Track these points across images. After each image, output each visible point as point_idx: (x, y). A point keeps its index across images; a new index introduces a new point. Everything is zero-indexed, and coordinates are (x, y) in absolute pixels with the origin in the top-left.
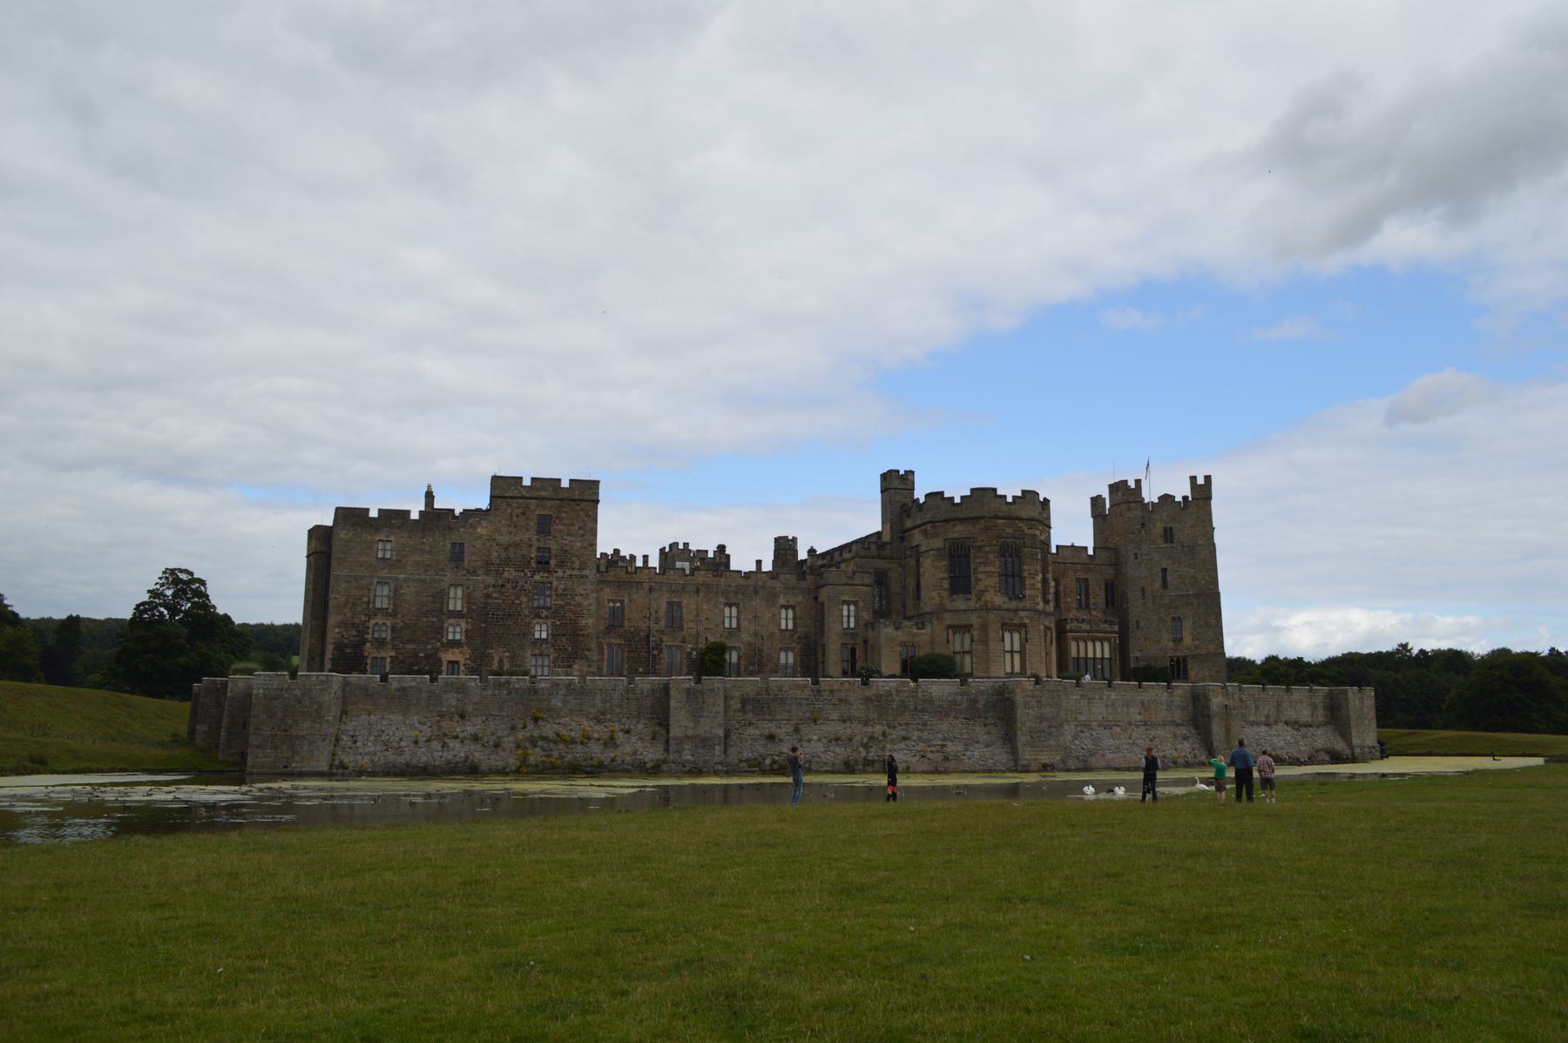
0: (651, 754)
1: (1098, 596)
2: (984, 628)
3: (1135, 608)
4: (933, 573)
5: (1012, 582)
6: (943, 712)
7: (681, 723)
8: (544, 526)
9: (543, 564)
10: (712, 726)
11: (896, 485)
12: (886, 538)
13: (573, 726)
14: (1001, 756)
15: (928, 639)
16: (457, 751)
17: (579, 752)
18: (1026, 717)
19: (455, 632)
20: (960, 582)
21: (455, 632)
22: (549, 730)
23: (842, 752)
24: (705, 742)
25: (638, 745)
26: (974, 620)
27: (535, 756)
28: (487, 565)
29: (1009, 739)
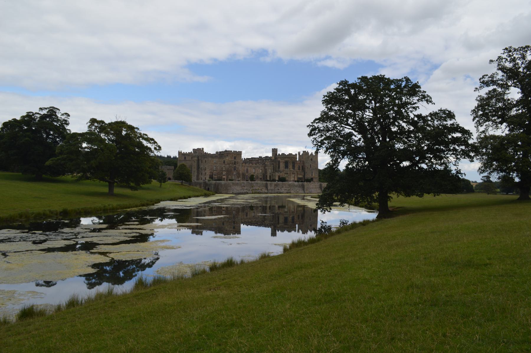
0: (266, 191)
1: (301, 169)
2: (290, 174)
3: (306, 170)
4: (282, 165)
5: (294, 167)
6: (296, 186)
7: (269, 188)
8: (235, 158)
9: (235, 163)
10: (273, 188)
11: (275, 151)
12: (273, 158)
13: (257, 188)
14: (303, 192)
15: (282, 175)
16: (245, 191)
17: (258, 191)
18: (306, 187)
19: (224, 173)
20: (287, 167)
21: (224, 173)
22: (254, 188)
23: (286, 191)
24: (272, 190)
25: (264, 190)
26: (289, 172)
27: (254, 191)
28: (228, 164)
29: (304, 190)
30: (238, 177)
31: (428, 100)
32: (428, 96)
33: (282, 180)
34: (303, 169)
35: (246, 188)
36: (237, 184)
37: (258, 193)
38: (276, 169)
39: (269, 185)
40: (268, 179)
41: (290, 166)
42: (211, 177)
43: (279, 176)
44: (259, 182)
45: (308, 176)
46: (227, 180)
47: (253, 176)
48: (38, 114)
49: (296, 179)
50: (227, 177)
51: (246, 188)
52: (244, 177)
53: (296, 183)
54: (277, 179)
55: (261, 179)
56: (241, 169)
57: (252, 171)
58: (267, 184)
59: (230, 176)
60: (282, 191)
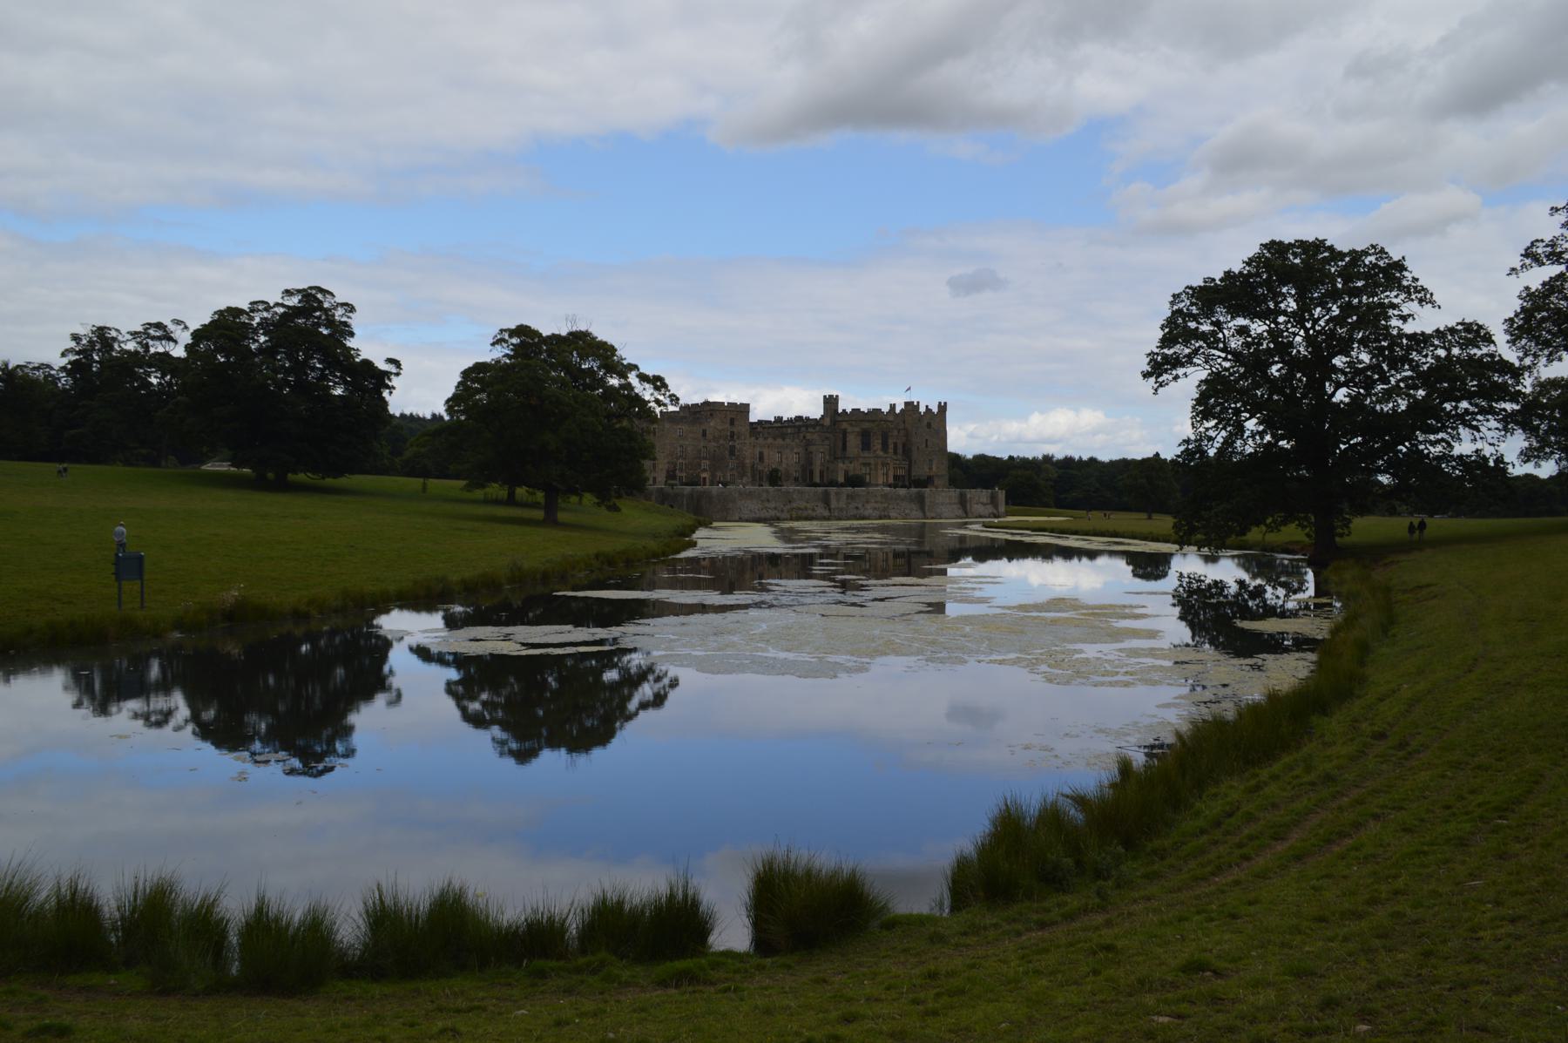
0: (826, 513)
1: (900, 451)
4: (853, 442)
7: (834, 504)
8: (732, 422)
10: (842, 504)
11: (831, 402)
12: (827, 422)
13: (803, 504)
14: (920, 514)
15: (855, 468)
16: (772, 513)
17: (805, 514)
18: (927, 501)
19: (705, 464)
20: (866, 446)
23: (877, 513)
24: (841, 510)
25: (821, 511)
29: (922, 508)
30: (742, 476)
31: (1425, 298)
32: (1423, 289)
33: (854, 481)
34: (907, 452)
35: (772, 505)
36: (750, 495)
37: (807, 519)
38: (839, 451)
39: (832, 497)
40: (817, 480)
41: (877, 444)
42: (671, 475)
43: (846, 472)
44: (792, 488)
45: (921, 471)
46: (712, 484)
47: (775, 471)
48: (282, 305)
49: (891, 480)
50: (713, 476)
51: (772, 505)
52: (757, 478)
53: (902, 491)
54: (841, 479)
55: (796, 479)
56: (748, 450)
57: (773, 459)
58: (827, 494)
59: (719, 474)
60: (866, 513)
